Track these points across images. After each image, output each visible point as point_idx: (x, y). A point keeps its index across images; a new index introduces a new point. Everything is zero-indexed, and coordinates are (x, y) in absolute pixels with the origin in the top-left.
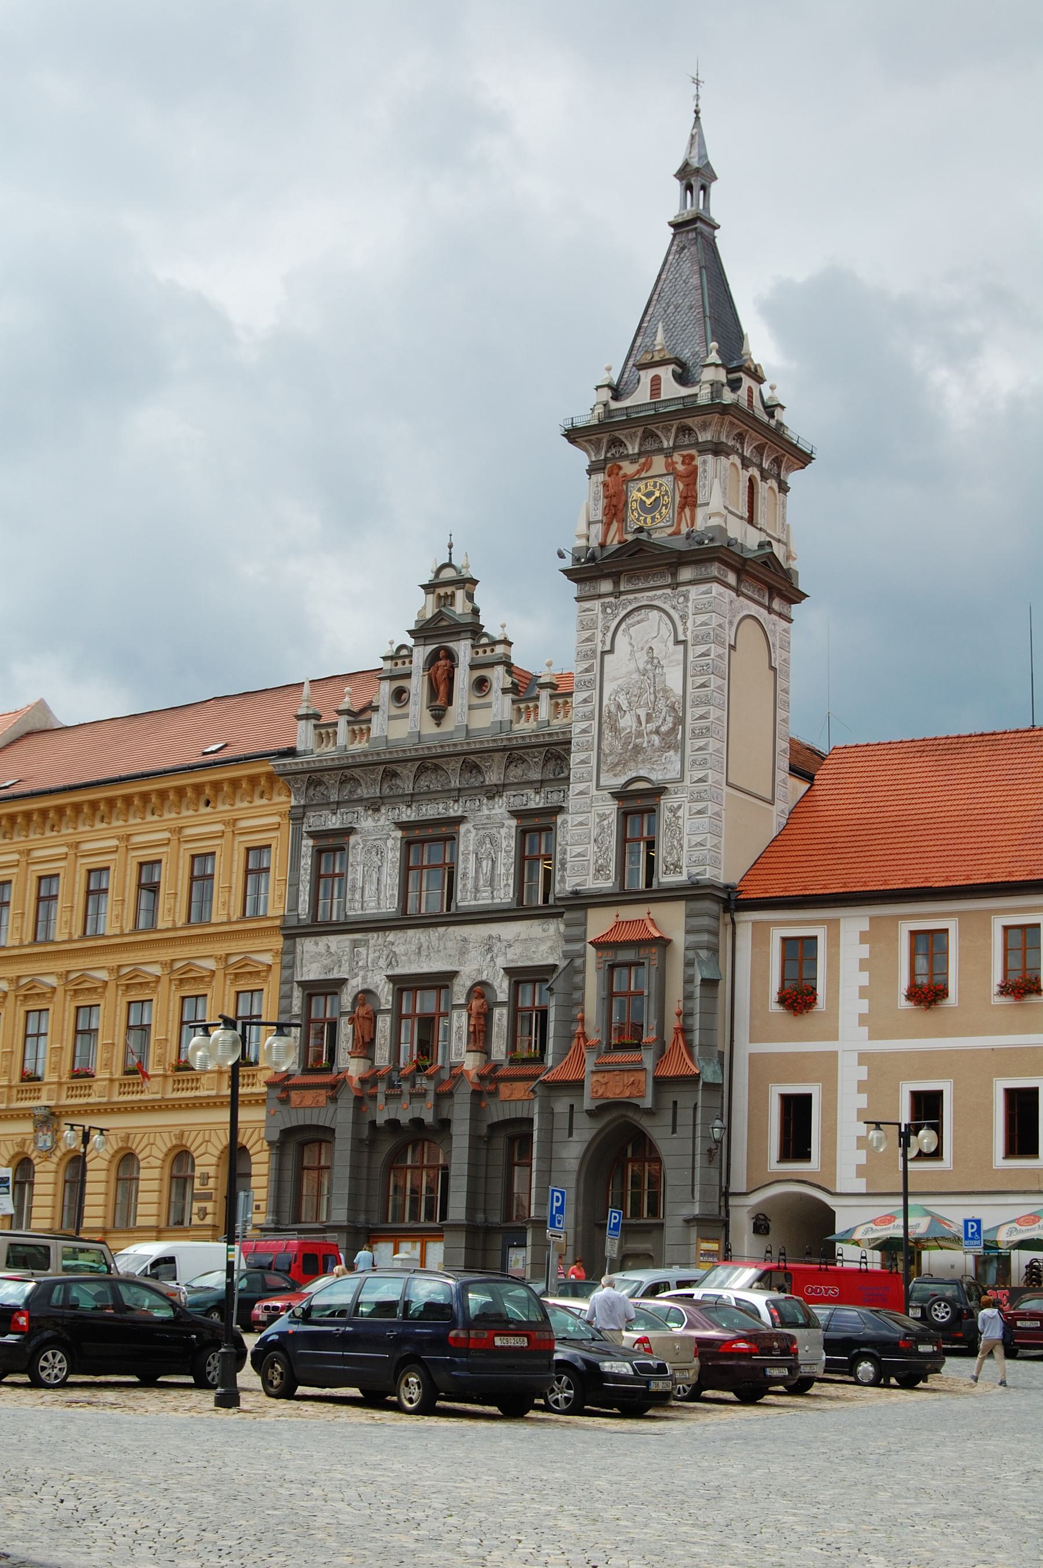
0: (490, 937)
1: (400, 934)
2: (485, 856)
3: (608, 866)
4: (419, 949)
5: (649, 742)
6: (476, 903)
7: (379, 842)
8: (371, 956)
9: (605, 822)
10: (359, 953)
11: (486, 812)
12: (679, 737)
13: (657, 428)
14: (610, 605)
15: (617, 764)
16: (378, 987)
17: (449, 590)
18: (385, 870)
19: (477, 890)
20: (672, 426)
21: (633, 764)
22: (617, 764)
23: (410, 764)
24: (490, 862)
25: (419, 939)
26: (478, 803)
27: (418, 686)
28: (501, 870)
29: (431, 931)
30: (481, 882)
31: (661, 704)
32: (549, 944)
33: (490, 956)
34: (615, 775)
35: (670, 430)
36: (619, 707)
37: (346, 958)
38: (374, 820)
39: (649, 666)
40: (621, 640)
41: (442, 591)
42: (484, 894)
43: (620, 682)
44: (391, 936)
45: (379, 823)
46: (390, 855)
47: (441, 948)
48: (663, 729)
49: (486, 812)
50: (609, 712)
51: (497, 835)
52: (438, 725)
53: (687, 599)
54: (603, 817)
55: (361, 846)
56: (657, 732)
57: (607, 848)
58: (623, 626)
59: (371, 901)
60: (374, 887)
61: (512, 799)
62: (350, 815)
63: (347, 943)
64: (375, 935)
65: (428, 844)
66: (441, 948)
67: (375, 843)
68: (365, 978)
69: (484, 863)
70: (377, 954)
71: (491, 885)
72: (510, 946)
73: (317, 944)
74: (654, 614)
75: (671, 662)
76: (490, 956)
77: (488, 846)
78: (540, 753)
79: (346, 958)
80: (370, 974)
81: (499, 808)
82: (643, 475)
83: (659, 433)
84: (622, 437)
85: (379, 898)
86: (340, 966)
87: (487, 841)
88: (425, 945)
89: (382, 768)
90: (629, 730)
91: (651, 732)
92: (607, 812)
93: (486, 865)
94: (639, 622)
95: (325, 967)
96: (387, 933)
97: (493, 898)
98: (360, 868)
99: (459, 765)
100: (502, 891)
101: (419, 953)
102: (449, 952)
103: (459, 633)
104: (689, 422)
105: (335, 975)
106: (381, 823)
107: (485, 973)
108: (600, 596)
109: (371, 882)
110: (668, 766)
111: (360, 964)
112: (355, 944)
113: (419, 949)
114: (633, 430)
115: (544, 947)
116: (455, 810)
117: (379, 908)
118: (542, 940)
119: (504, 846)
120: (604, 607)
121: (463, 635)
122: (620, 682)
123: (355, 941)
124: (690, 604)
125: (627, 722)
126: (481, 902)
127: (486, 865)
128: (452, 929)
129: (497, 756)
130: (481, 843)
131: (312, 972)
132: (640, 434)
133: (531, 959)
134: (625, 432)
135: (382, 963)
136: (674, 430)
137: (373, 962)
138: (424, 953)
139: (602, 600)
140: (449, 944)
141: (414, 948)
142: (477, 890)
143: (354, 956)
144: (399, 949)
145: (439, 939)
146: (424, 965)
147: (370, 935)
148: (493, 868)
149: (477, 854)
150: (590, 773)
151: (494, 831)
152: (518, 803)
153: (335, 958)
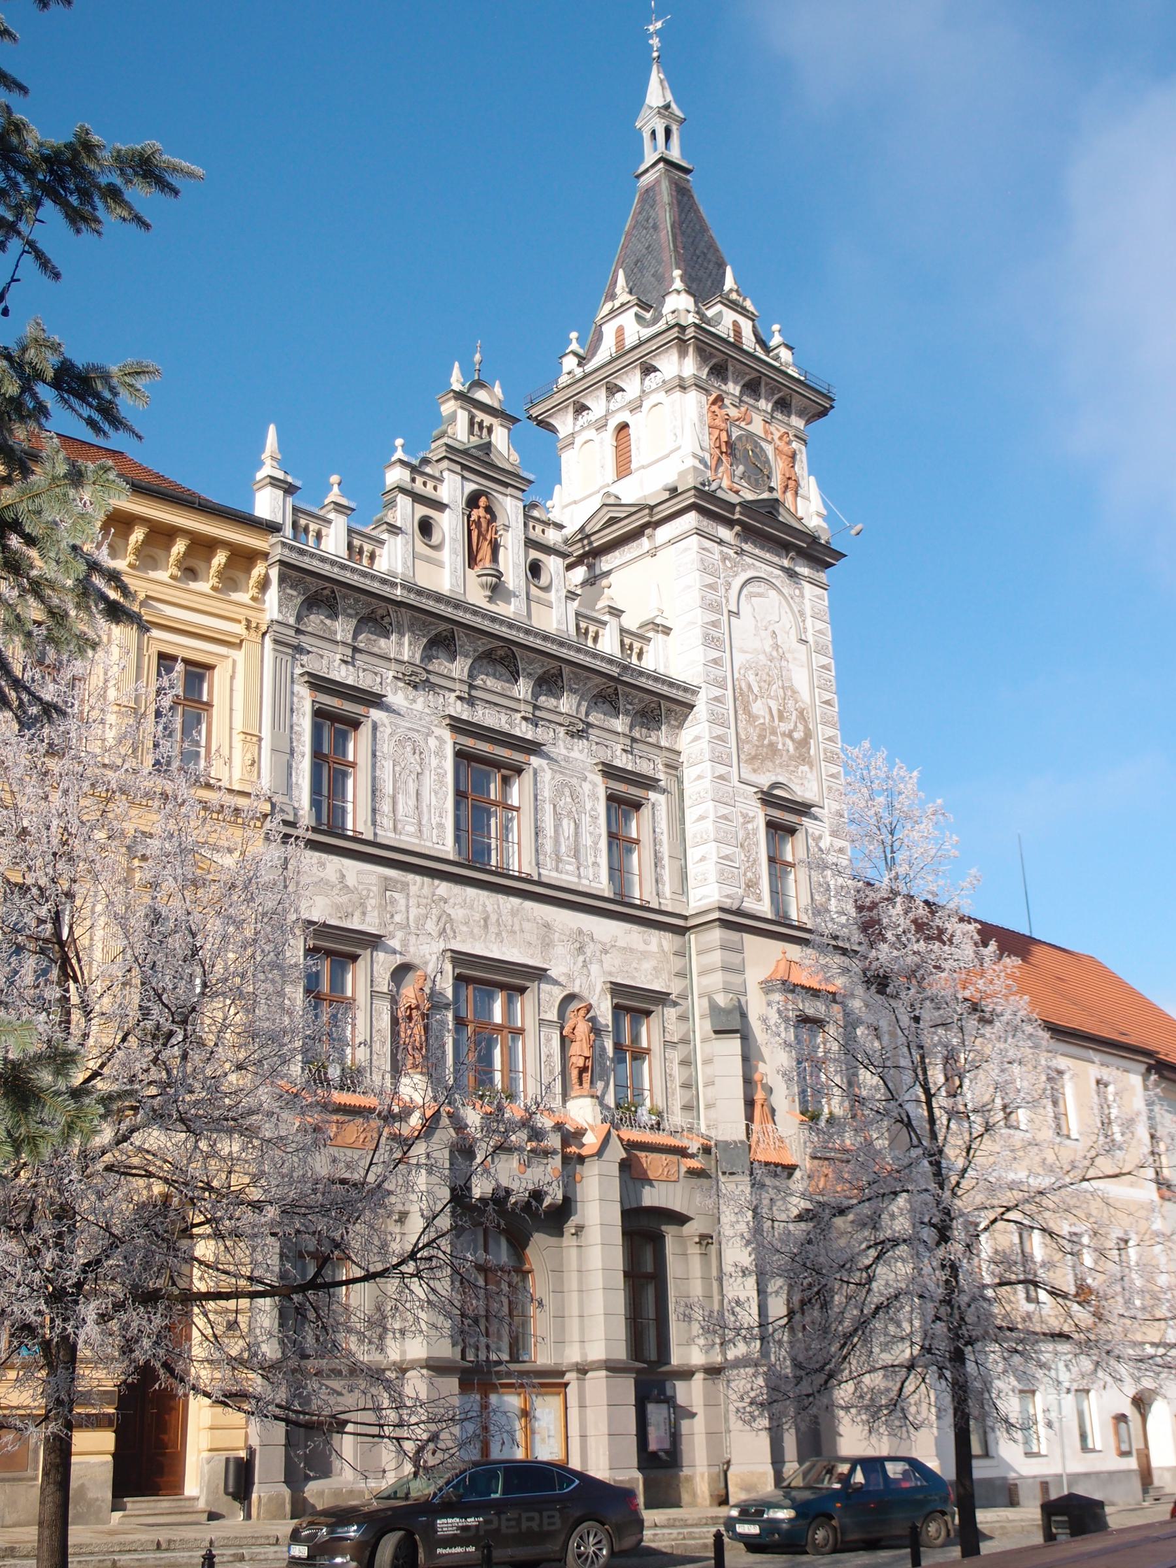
0: (580, 932)
1: (456, 889)
2: (555, 813)
3: (757, 884)
4: (486, 920)
5: (784, 745)
6: (559, 876)
7: (415, 735)
8: (414, 912)
9: (750, 826)
10: (393, 902)
11: (564, 752)
12: (812, 752)
13: (767, 384)
14: (729, 559)
15: (755, 758)
16: (426, 963)
17: (488, 420)
18: (428, 781)
19: (558, 859)
20: (780, 391)
21: (770, 764)
22: (755, 758)
23: (485, 640)
24: (572, 825)
25: (484, 906)
26: (552, 734)
27: (449, 524)
28: (586, 840)
29: (501, 898)
30: (563, 849)
31: (791, 703)
32: (653, 963)
33: (581, 958)
34: (755, 771)
35: (773, 394)
36: (750, 687)
37: (372, 902)
38: (407, 698)
39: (775, 654)
40: (745, 609)
41: (480, 416)
42: (568, 867)
43: (748, 656)
44: (443, 888)
45: (414, 706)
46: (434, 762)
47: (516, 928)
48: (796, 735)
49: (564, 752)
50: (741, 689)
51: (579, 789)
52: (491, 599)
53: (802, 596)
54: (748, 819)
55: (389, 731)
56: (790, 736)
57: (755, 861)
58: (745, 592)
59: (408, 823)
60: (412, 802)
61: (594, 747)
62: (370, 676)
63: (373, 879)
64: (418, 878)
65: (485, 765)
66: (516, 928)
67: (411, 734)
68: (405, 943)
69: (565, 822)
70: (423, 911)
71: (576, 856)
72: (606, 952)
73: (322, 865)
74: (773, 593)
75: (795, 659)
76: (581, 958)
77: (569, 800)
78: (641, 701)
79: (372, 902)
80: (413, 939)
81: (581, 754)
82: (743, 424)
83: (763, 390)
84: (730, 368)
85: (420, 823)
86: (364, 914)
87: (567, 792)
88: (493, 918)
89: (444, 626)
90: (762, 721)
91: (783, 734)
92: (751, 814)
93: (567, 827)
94: (760, 595)
95: (338, 907)
96: (437, 882)
97: (579, 876)
98: (388, 765)
99: (540, 671)
100: (591, 870)
101: (486, 926)
102: (527, 936)
103: (506, 485)
104: (796, 401)
105: (355, 924)
106: (419, 705)
107: (577, 983)
108: (721, 542)
109: (406, 793)
110: (806, 782)
111: (397, 918)
112: (387, 885)
113: (486, 920)
114: (748, 370)
115: (647, 965)
116: (523, 730)
117: (420, 838)
118: (645, 955)
119: (588, 807)
120: (725, 558)
121: (510, 490)
122: (748, 656)
123: (386, 878)
124: (806, 601)
125: (758, 708)
126: (564, 877)
127: (567, 827)
128: (529, 904)
129: (598, 680)
130: (558, 792)
131: (319, 910)
132: (747, 378)
133: (633, 978)
134: (739, 366)
135: (431, 926)
136: (776, 397)
137: (417, 919)
138: (493, 929)
139: (724, 549)
140: (527, 926)
141: (477, 917)
142: (558, 859)
143: (386, 905)
144: (457, 913)
145: (514, 913)
146: (495, 948)
147: (410, 877)
148: (577, 834)
149: (555, 806)
150: (730, 755)
151: (574, 781)
152: (605, 755)
153: (355, 897)
